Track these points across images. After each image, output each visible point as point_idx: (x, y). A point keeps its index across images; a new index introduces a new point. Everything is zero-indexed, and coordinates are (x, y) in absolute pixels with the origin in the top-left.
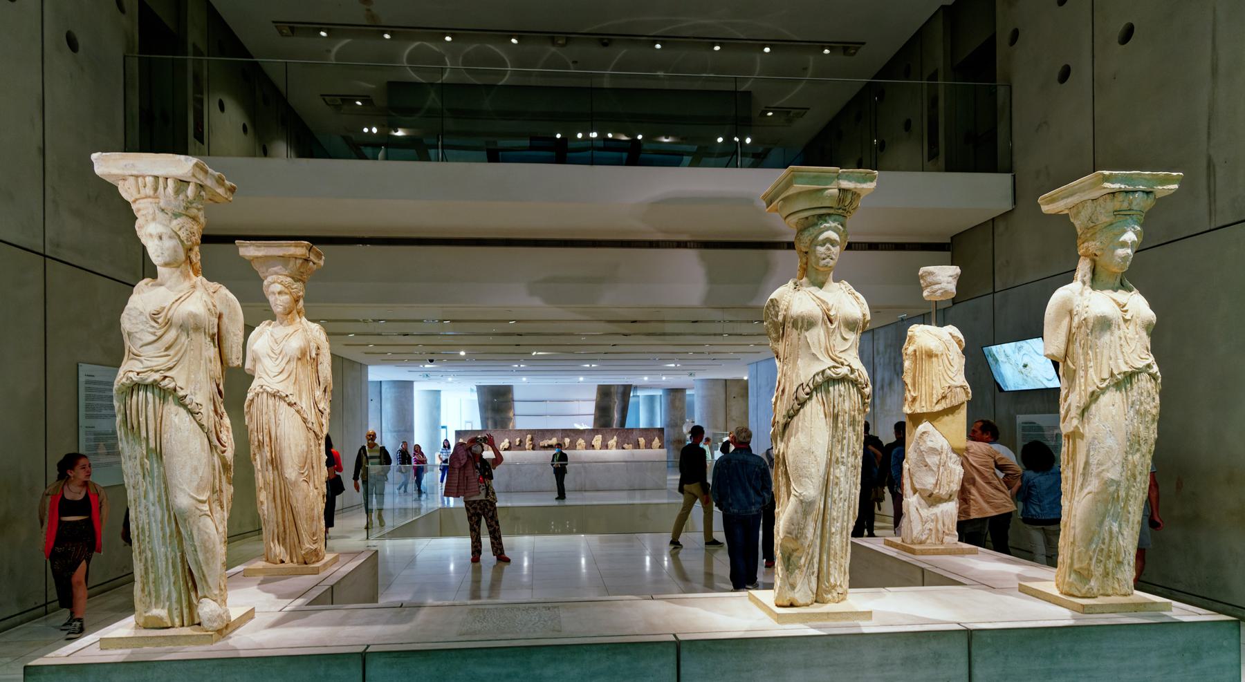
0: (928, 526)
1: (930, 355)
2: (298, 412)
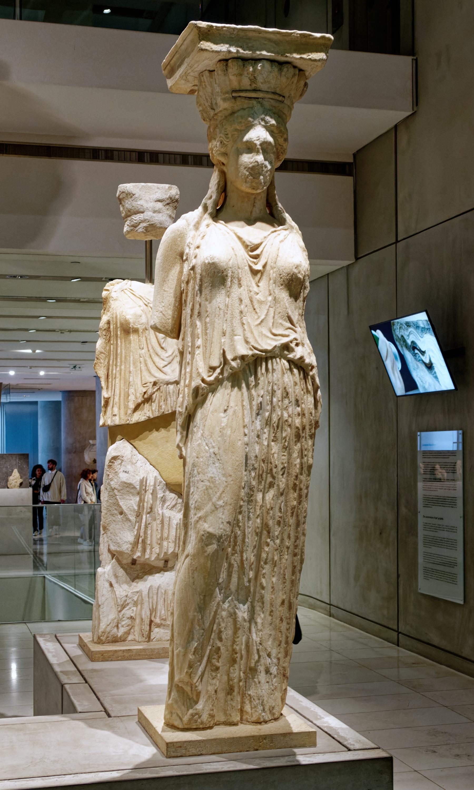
0: (128, 612)
1: (127, 330)
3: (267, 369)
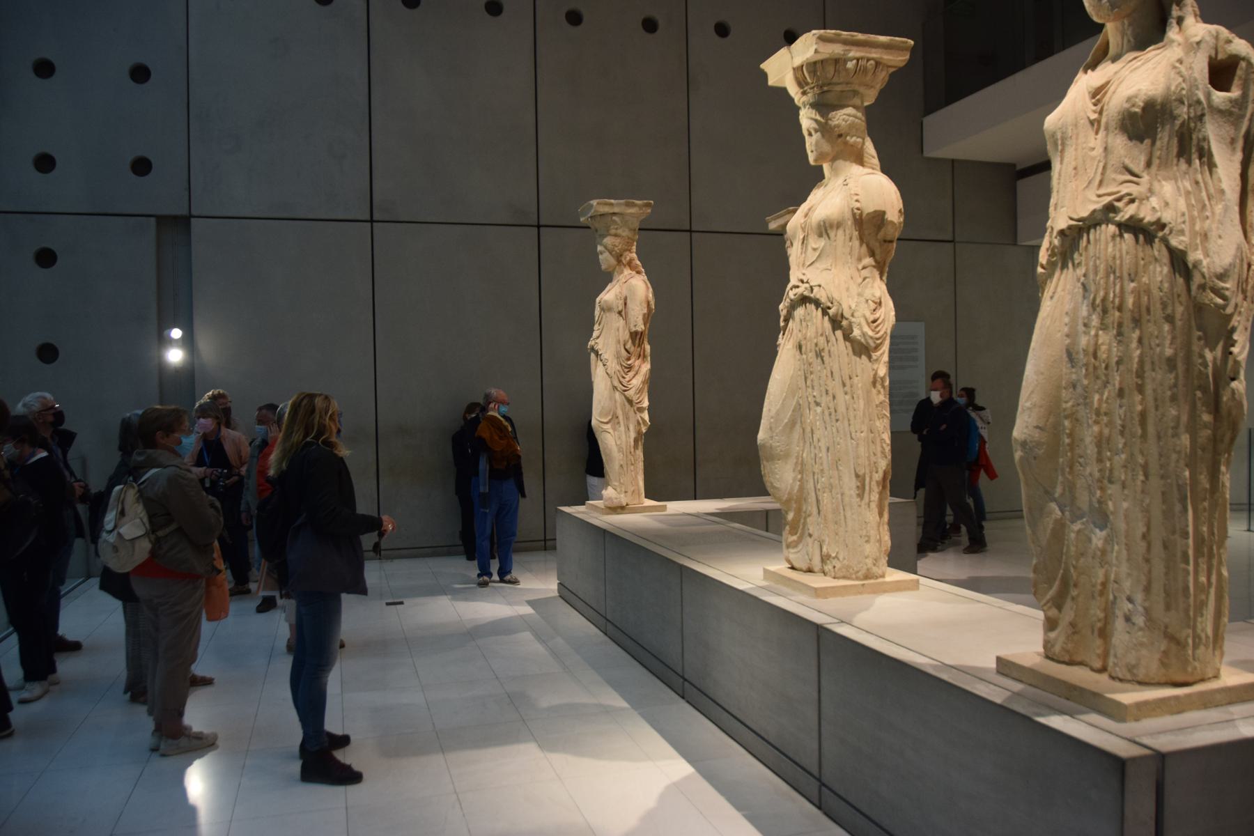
3: (1089, 241)
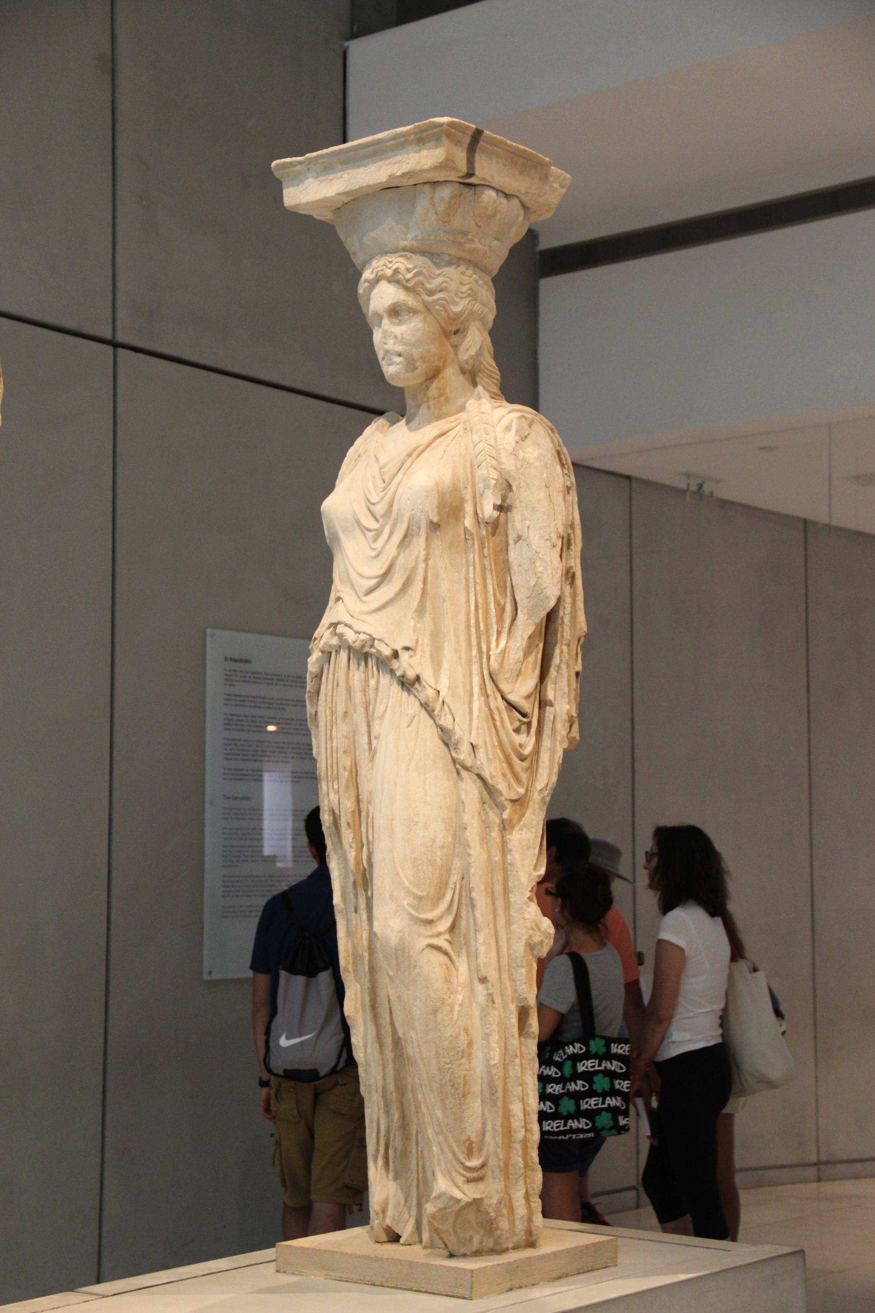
2: (425, 706)
